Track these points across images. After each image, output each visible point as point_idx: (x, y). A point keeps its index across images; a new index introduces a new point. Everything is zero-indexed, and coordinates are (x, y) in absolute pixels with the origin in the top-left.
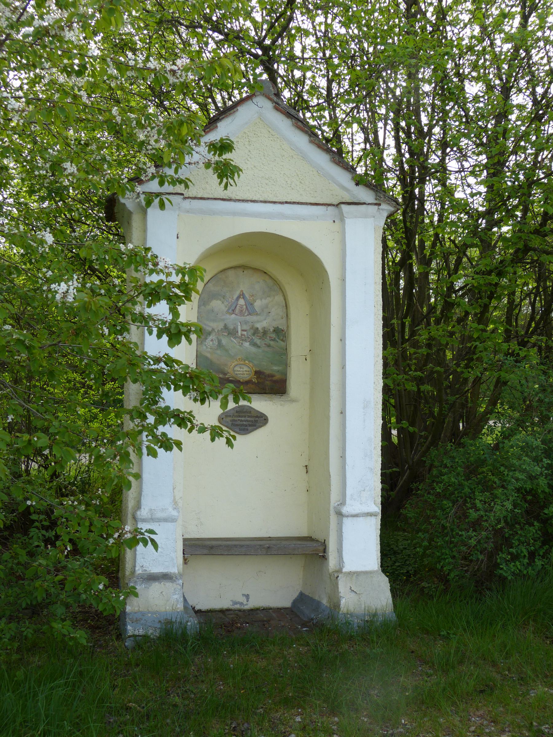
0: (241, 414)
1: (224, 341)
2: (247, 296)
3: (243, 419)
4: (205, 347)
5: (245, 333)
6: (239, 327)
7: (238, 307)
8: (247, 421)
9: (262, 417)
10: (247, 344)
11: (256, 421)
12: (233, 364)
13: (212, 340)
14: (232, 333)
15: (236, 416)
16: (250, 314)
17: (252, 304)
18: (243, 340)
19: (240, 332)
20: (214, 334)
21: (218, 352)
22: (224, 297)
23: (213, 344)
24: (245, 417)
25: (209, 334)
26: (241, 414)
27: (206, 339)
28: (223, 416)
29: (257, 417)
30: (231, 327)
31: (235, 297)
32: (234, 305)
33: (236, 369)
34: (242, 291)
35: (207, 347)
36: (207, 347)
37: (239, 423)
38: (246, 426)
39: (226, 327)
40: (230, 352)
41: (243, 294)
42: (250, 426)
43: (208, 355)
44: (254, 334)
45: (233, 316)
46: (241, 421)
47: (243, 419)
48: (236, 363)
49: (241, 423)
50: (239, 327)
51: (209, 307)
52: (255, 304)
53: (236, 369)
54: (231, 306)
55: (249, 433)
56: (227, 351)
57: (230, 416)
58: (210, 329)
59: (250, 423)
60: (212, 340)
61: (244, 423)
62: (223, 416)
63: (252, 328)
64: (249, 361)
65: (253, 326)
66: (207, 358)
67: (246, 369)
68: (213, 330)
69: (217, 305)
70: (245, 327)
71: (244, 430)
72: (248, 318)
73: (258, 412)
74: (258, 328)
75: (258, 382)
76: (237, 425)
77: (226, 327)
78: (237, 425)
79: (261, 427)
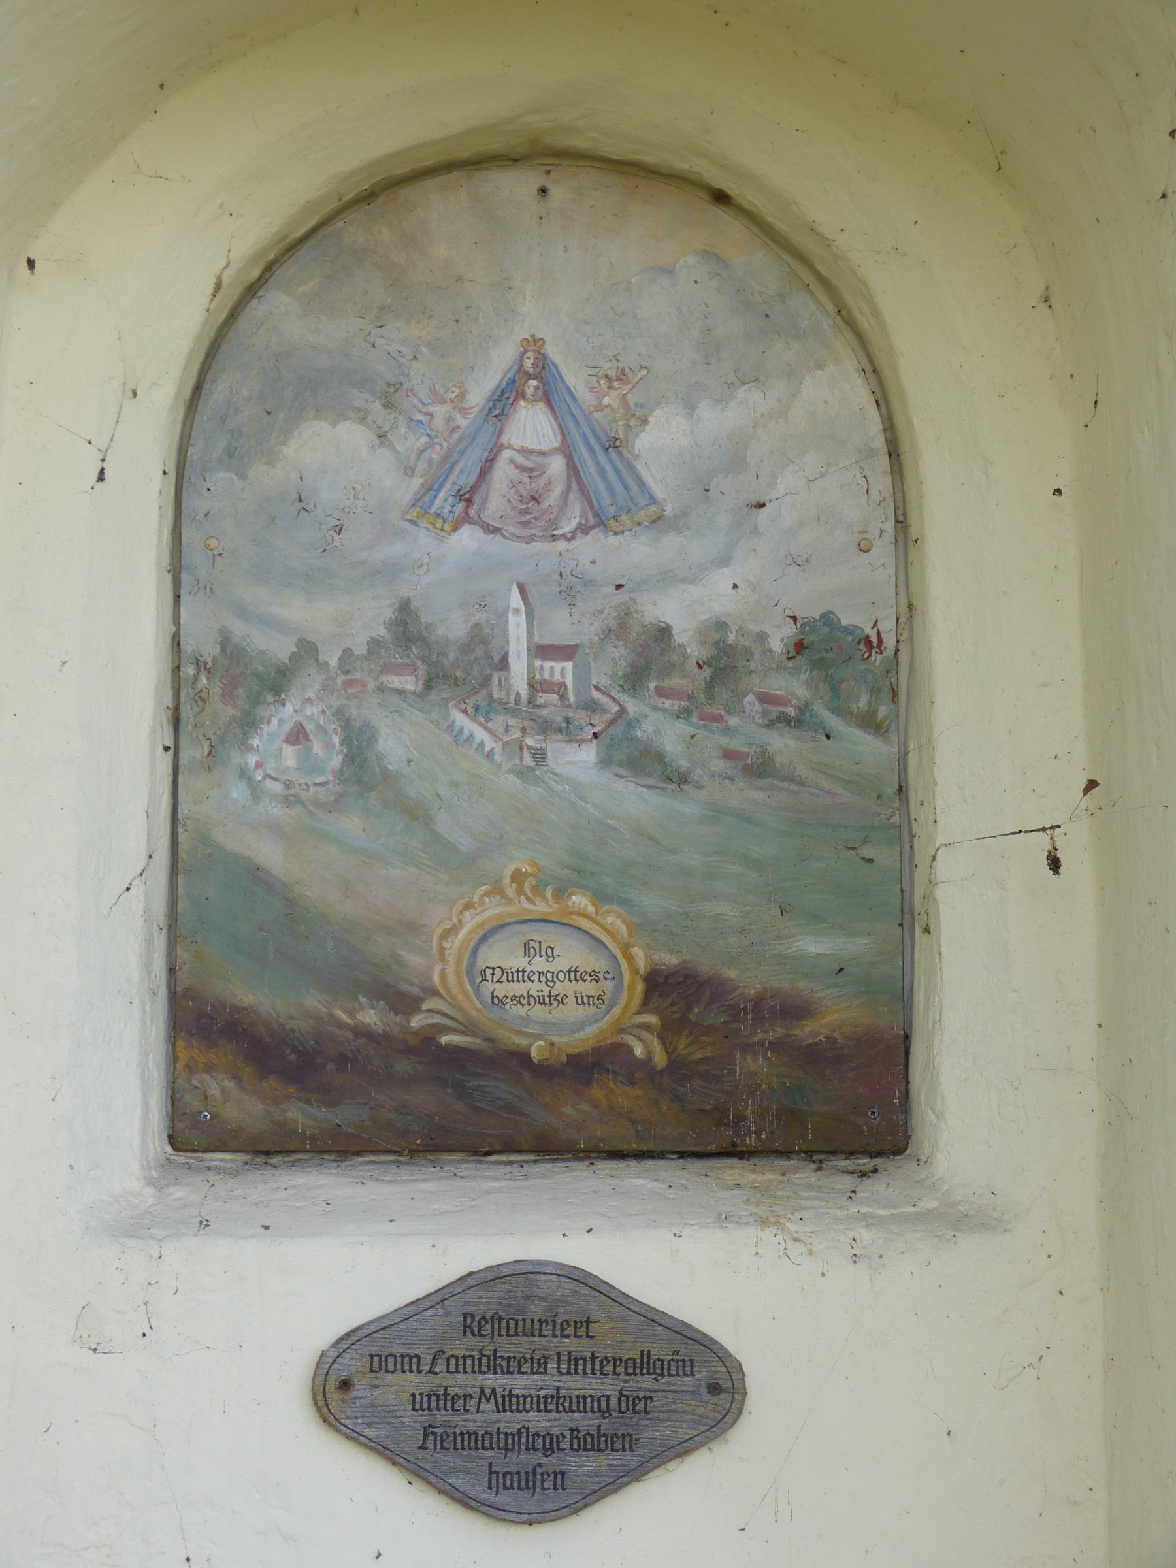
0: (505, 1346)
1: (396, 740)
2: (575, 378)
3: (521, 1383)
4: (238, 792)
5: (562, 671)
6: (517, 626)
7: (503, 472)
8: (559, 1401)
9: (686, 1367)
10: (578, 761)
11: (638, 1404)
12: (471, 923)
13: (298, 736)
14: (454, 670)
15: (461, 1364)
16: (599, 520)
17: (613, 445)
18: (545, 728)
19: (519, 665)
20: (310, 684)
21: (351, 825)
22: (391, 395)
23: (309, 765)
24: (540, 1365)
25: (277, 682)
26: (505, 1346)
27: (250, 724)
28: (353, 1363)
29: (645, 1364)
30: (451, 625)
31: (479, 393)
32: (473, 459)
33: (491, 956)
34: (534, 343)
35: (256, 792)
36: (256, 792)
37: (486, 1418)
38: (551, 1444)
39: (407, 628)
40: (443, 824)
41: (544, 370)
42: (582, 1442)
43: (269, 854)
44: (634, 679)
45: (468, 538)
46: (507, 1401)
47: (521, 1383)
48: (493, 910)
49: (510, 1421)
50: (517, 626)
51: (266, 477)
52: (643, 442)
53: (491, 956)
54: (449, 461)
55: (575, 1508)
56: (416, 814)
57: (410, 1362)
58: (281, 648)
59: (587, 1422)
60: (298, 736)
61: (536, 1420)
62: (353, 1363)
63: (620, 626)
64: (600, 897)
65: (626, 614)
66: (255, 876)
67: (572, 954)
68: (307, 650)
69: (335, 455)
70: (561, 626)
71: (530, 1481)
72: (590, 552)
73: (653, 1318)
74: (664, 633)
75: (675, 1066)
76: (473, 1441)
77: (407, 628)
78: (473, 1441)
79: (681, 1450)
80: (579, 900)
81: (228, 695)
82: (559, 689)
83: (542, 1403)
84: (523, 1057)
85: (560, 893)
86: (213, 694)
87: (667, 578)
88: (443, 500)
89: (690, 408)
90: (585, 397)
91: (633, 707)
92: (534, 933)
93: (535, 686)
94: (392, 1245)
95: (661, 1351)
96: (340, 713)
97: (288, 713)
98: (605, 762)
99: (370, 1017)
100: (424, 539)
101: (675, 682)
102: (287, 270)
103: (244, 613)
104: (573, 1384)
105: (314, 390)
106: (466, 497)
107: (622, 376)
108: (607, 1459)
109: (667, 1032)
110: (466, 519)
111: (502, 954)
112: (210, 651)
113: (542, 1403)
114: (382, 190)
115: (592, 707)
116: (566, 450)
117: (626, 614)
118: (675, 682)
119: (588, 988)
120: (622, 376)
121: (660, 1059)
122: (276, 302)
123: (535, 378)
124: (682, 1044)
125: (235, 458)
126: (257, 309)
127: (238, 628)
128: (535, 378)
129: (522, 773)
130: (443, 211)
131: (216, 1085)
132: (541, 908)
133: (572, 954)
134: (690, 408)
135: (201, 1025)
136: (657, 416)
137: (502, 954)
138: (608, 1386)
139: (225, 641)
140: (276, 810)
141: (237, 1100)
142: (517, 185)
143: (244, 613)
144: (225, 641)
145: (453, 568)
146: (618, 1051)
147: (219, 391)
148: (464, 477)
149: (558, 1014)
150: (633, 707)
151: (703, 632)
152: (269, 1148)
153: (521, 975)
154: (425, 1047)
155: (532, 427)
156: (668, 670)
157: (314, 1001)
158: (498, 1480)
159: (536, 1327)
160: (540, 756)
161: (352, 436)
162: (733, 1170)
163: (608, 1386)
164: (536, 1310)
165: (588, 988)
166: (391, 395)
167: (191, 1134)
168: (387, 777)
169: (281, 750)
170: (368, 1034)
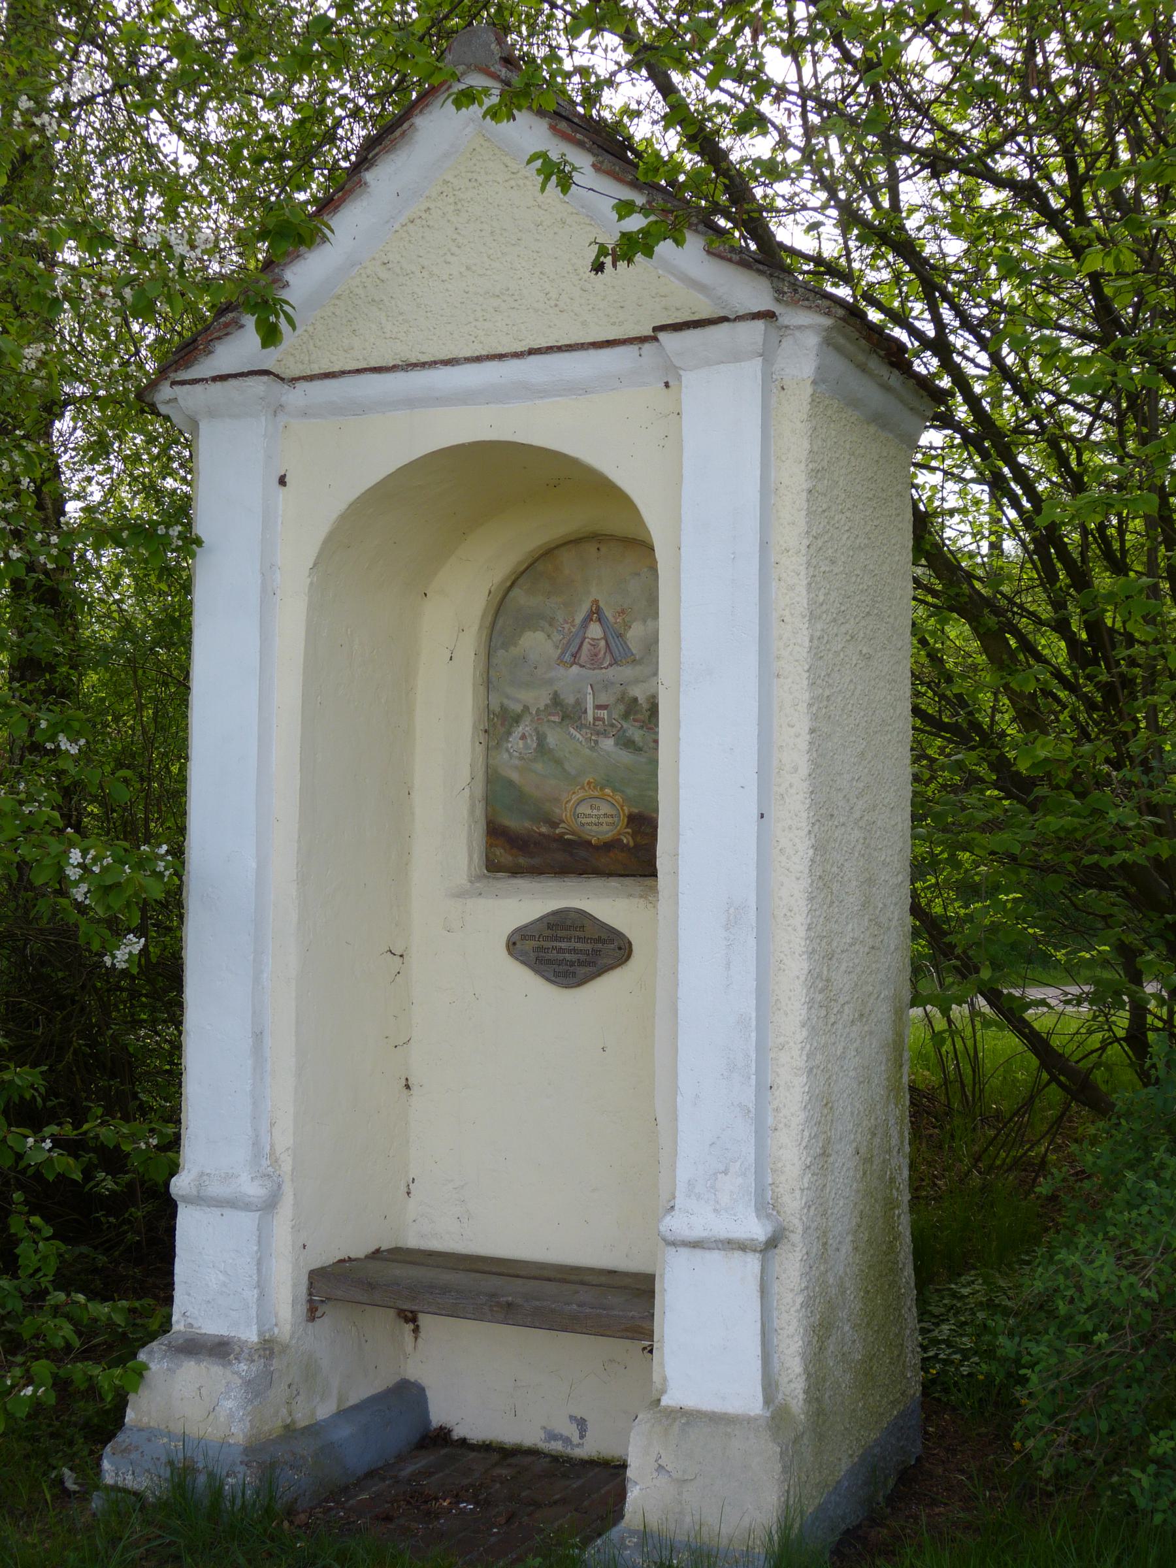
0: (560, 933)
1: (552, 740)
2: (609, 613)
3: (563, 945)
4: (506, 756)
5: (604, 714)
6: (590, 699)
7: (586, 646)
8: (574, 951)
9: (612, 941)
10: (608, 744)
11: (597, 952)
12: (575, 798)
13: (523, 737)
15: (547, 938)
16: (615, 662)
17: (620, 636)
18: (598, 734)
19: (590, 712)
20: (527, 720)
21: (539, 766)
22: (552, 622)
23: (526, 747)
24: (569, 939)
25: (517, 719)
26: (560, 933)
27: (509, 733)
28: (516, 938)
29: (599, 940)
30: (570, 700)
31: (578, 621)
32: (578, 641)
33: (580, 810)
34: (596, 601)
35: (510, 755)
36: (510, 755)
37: (553, 955)
38: (572, 964)
39: (556, 701)
40: (567, 766)
42: (581, 963)
43: (514, 776)
44: (626, 716)
45: (575, 669)
46: (560, 950)
47: (563, 945)
48: (581, 794)
49: (561, 956)
50: (590, 699)
51: (514, 651)
52: (630, 634)
53: (580, 810)
54: (569, 644)
55: (580, 984)
56: (558, 762)
57: (532, 937)
58: (518, 708)
59: (583, 957)
60: (523, 737)
61: (568, 956)
62: (516, 938)
63: (621, 699)
64: (614, 790)
65: (624, 694)
66: (510, 783)
67: (605, 809)
68: (526, 708)
69: (537, 644)
70: (603, 699)
71: (566, 975)
72: (612, 673)
73: (604, 926)
74: (636, 700)
75: (636, 846)
76: (550, 962)
77: (556, 701)
78: (550, 962)
79: (611, 968)
80: (608, 791)
81: (503, 725)
82: (602, 720)
83: (570, 951)
84: (589, 843)
85: (602, 789)
86: (497, 724)
87: (637, 681)
88: (567, 657)
89: (645, 621)
90: (612, 620)
91: (625, 725)
92: (593, 802)
93: (595, 719)
94: (531, 902)
95: (604, 936)
96: (536, 729)
97: (519, 730)
98: (616, 744)
99: (544, 829)
100: (561, 671)
101: (639, 716)
102: (521, 581)
103: (508, 697)
104: (579, 946)
105: (528, 621)
106: (574, 655)
107: (623, 612)
108: (588, 969)
109: (634, 835)
110: (574, 663)
111: (584, 809)
112: (497, 710)
113: (570, 951)
114: (548, 553)
115: (612, 725)
116: (605, 638)
117: (624, 694)
118: (639, 716)
119: (610, 820)
120: (623, 612)
121: (632, 844)
122: (516, 592)
123: (596, 614)
124: (638, 839)
125: (505, 646)
126: (511, 594)
127: (506, 702)
128: (596, 614)
129: (592, 749)
130: (567, 558)
131: (499, 851)
132: (596, 794)
133: (605, 809)
134: (645, 621)
135: (495, 832)
136: (634, 625)
137: (584, 809)
138: (589, 947)
139: (502, 706)
140: (517, 762)
141: (503, 855)
142: (591, 548)
143: (508, 697)
144: (502, 706)
145: (571, 680)
146: (620, 840)
147: (500, 623)
148: (573, 649)
149: (601, 829)
150: (625, 725)
151: (648, 700)
152: (515, 871)
153: (590, 816)
154: (560, 839)
155: (595, 630)
156: (636, 713)
157: (527, 824)
158: (557, 974)
159: (568, 928)
160: (596, 742)
161: (540, 636)
162: (628, 881)
163: (589, 947)
164: (569, 923)
165: (610, 820)
166: (552, 622)
167: (493, 867)
168: (550, 751)
169: (518, 742)
170: (540, 834)
